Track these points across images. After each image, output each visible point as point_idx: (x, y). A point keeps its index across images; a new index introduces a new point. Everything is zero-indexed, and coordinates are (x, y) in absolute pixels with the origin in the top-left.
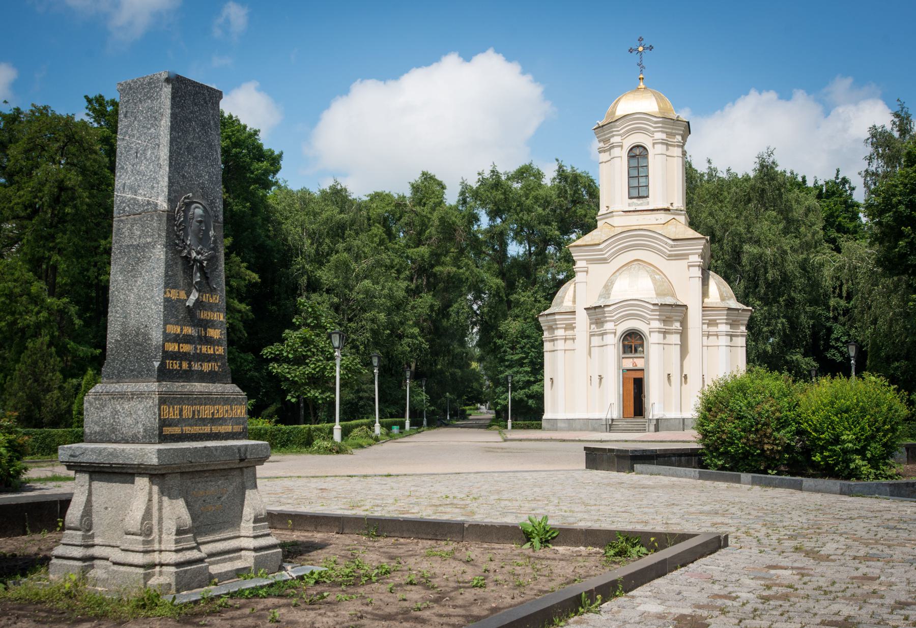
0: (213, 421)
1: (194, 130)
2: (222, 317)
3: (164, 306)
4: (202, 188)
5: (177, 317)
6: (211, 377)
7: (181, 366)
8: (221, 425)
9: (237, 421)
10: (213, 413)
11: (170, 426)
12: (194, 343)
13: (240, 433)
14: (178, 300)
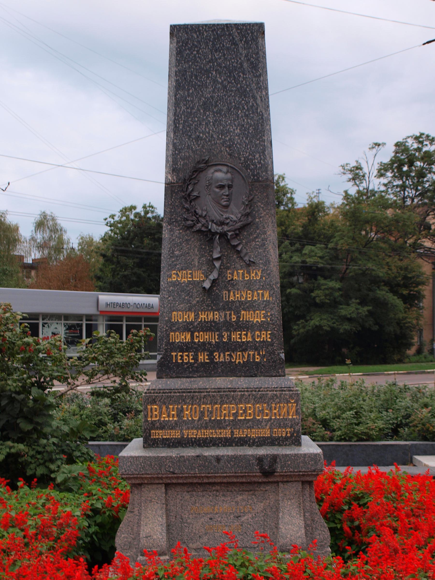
0: (235, 424)
1: (215, 81)
2: (267, 295)
3: (169, 292)
4: (229, 147)
5: (189, 301)
6: (249, 370)
7: (196, 358)
8: (251, 428)
9: (282, 424)
10: (236, 415)
11: (162, 427)
12: (218, 330)
13: (286, 438)
14: (193, 283)
